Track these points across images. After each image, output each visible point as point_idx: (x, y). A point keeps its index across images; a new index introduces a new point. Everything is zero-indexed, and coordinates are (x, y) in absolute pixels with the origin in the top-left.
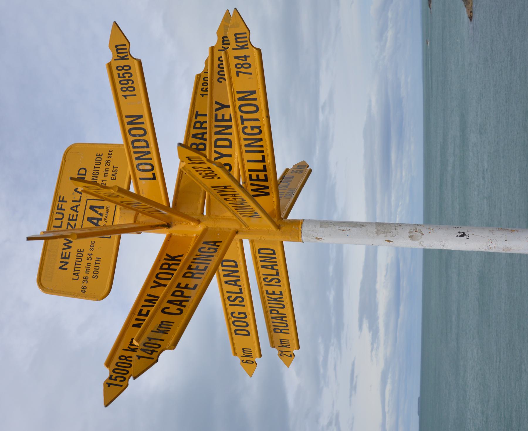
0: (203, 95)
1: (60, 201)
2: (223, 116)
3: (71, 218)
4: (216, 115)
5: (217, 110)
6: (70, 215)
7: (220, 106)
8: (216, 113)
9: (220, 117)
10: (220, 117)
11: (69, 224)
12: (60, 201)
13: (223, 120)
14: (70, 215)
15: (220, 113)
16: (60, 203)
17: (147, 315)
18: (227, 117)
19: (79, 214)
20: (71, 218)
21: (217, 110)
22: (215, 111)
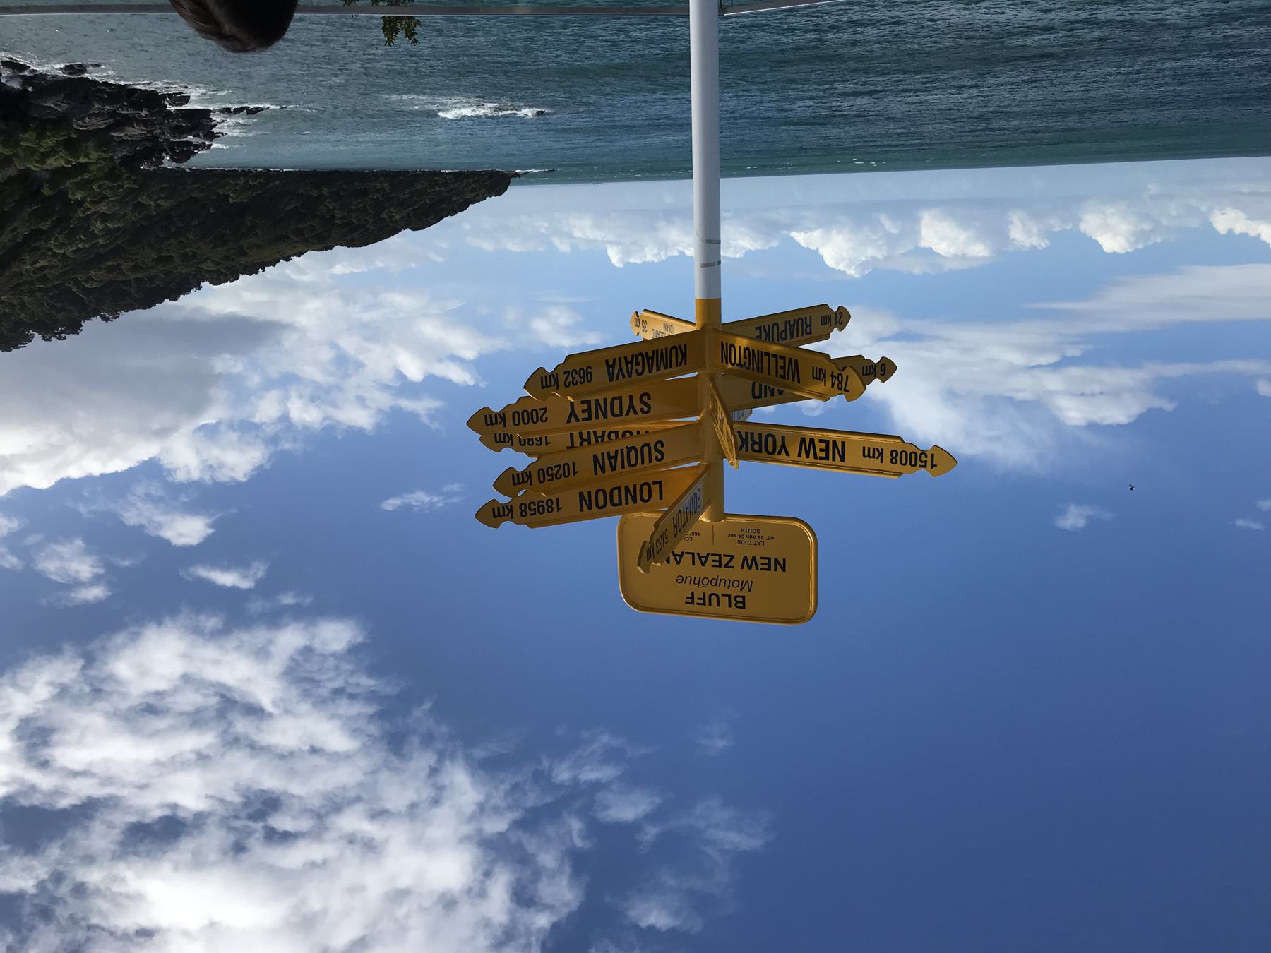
0: (547, 443)
1: (693, 603)
2: (583, 411)
3: (717, 564)
4: (584, 420)
5: (577, 420)
6: (713, 566)
7: (573, 417)
8: (581, 420)
9: (586, 415)
10: (586, 415)
11: (726, 566)
12: (693, 603)
13: (589, 411)
14: (713, 566)
15: (581, 416)
16: (696, 601)
17: (827, 442)
18: (585, 406)
19: (711, 553)
20: (717, 564)
21: (577, 420)
22: (579, 421)
